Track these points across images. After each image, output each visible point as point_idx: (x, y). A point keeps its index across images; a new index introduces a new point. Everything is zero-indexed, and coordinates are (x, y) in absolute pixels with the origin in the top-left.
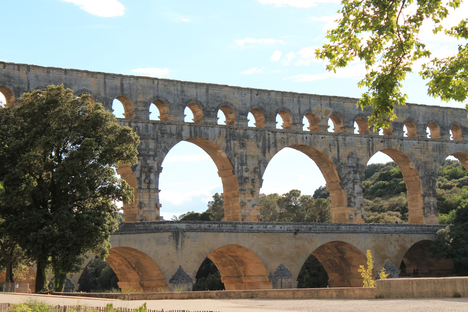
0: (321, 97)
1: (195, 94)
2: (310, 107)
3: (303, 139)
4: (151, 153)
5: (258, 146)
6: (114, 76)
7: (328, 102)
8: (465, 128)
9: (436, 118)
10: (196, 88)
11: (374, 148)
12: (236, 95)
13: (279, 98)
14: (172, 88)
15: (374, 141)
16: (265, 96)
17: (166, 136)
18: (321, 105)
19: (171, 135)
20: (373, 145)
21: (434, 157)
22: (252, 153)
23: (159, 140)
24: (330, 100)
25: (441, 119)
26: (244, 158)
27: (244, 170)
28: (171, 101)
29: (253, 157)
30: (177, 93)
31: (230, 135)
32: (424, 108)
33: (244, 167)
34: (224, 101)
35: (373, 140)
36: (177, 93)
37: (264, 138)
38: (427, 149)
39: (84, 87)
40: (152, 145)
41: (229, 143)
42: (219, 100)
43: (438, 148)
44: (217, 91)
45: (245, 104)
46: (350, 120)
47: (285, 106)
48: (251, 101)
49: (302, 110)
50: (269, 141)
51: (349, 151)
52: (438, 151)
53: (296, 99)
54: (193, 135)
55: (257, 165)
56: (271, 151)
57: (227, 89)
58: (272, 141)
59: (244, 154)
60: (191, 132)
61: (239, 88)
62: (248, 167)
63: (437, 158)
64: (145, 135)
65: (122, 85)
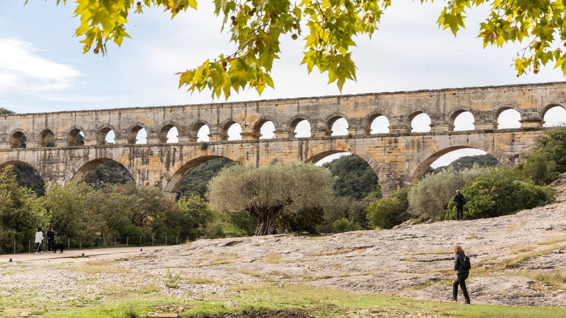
0: (245, 103)
1: (108, 120)
2: (232, 116)
3: (214, 150)
4: (61, 174)
5: (162, 161)
6: (40, 114)
7: (255, 107)
8: (479, 112)
9: (423, 106)
10: (109, 114)
11: (309, 151)
12: (149, 114)
13: (195, 112)
14: (88, 118)
15: (309, 144)
16: (180, 112)
17: (74, 159)
18: (246, 111)
19: (79, 157)
20: (307, 149)
21: (407, 156)
22: (155, 168)
23: (68, 163)
24: (258, 105)
25: (433, 106)
26: (146, 173)
27: (145, 184)
28: (86, 128)
29: (155, 171)
30: (91, 120)
31: (133, 152)
32: (403, 95)
33: (145, 182)
34: (135, 121)
35: (307, 143)
36: (91, 120)
37: (169, 152)
38: (396, 147)
39: (18, 127)
40: (62, 167)
41: (132, 161)
42: (130, 121)
43: (416, 144)
44: (129, 114)
45: (157, 122)
46: (283, 124)
47: (201, 118)
48: (164, 118)
49: (221, 121)
50: (174, 155)
51: (272, 157)
52: (416, 147)
53: (214, 110)
54: (98, 156)
55: (159, 179)
56: (175, 164)
57: (139, 110)
58: (177, 155)
59: (147, 169)
60: (96, 154)
61: (151, 108)
62: (149, 181)
63: (413, 156)
64: (57, 160)
65: (46, 121)
